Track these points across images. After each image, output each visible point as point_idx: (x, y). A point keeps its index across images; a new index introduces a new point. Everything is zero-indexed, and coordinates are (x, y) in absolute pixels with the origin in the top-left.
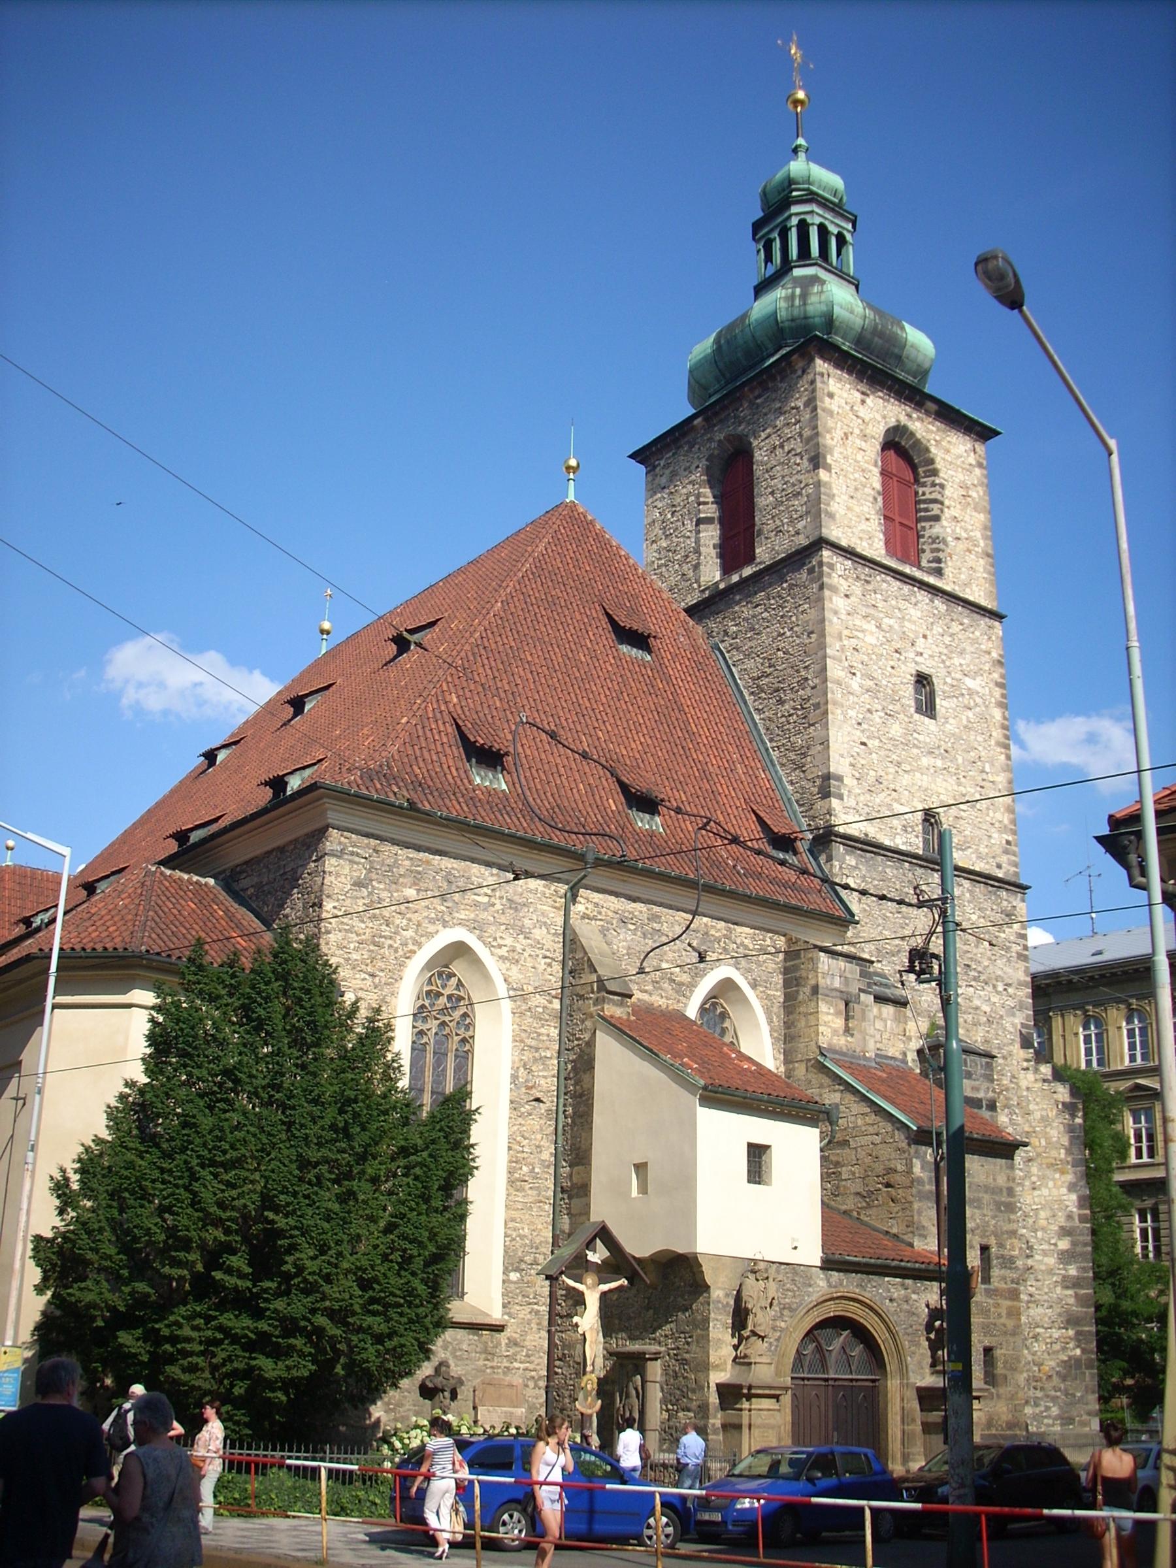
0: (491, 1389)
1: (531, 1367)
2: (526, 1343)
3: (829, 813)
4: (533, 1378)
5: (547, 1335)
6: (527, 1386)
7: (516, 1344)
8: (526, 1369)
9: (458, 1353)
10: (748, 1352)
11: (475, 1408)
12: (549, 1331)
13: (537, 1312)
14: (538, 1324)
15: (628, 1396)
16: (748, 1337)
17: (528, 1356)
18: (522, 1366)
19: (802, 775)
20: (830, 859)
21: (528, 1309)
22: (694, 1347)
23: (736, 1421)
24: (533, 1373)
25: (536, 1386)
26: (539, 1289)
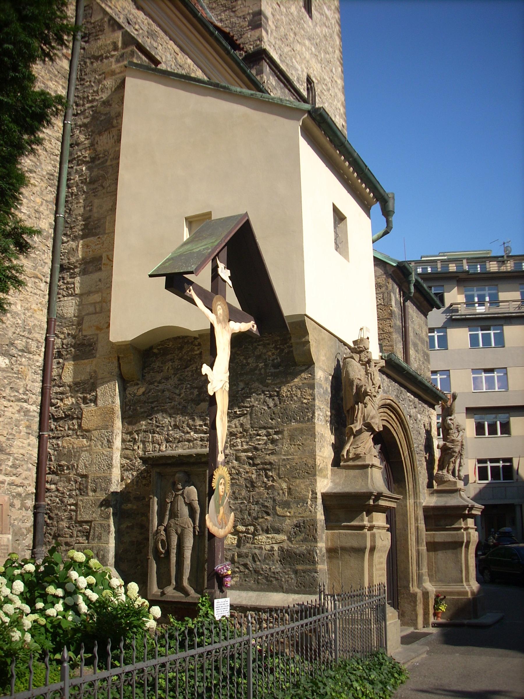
1: (18, 481)
2: (14, 450)
3: (260, 39)
4: (19, 495)
5: (35, 441)
6: (12, 505)
8: (12, 484)
10: (359, 451)
12: (40, 437)
13: (27, 412)
14: (28, 427)
15: (174, 515)
16: (360, 432)
17: (14, 466)
18: (8, 479)
19: (232, 14)
20: (260, 72)
21: (16, 406)
22: (285, 446)
23: (354, 543)
24: (20, 490)
25: (23, 506)
26: (30, 384)
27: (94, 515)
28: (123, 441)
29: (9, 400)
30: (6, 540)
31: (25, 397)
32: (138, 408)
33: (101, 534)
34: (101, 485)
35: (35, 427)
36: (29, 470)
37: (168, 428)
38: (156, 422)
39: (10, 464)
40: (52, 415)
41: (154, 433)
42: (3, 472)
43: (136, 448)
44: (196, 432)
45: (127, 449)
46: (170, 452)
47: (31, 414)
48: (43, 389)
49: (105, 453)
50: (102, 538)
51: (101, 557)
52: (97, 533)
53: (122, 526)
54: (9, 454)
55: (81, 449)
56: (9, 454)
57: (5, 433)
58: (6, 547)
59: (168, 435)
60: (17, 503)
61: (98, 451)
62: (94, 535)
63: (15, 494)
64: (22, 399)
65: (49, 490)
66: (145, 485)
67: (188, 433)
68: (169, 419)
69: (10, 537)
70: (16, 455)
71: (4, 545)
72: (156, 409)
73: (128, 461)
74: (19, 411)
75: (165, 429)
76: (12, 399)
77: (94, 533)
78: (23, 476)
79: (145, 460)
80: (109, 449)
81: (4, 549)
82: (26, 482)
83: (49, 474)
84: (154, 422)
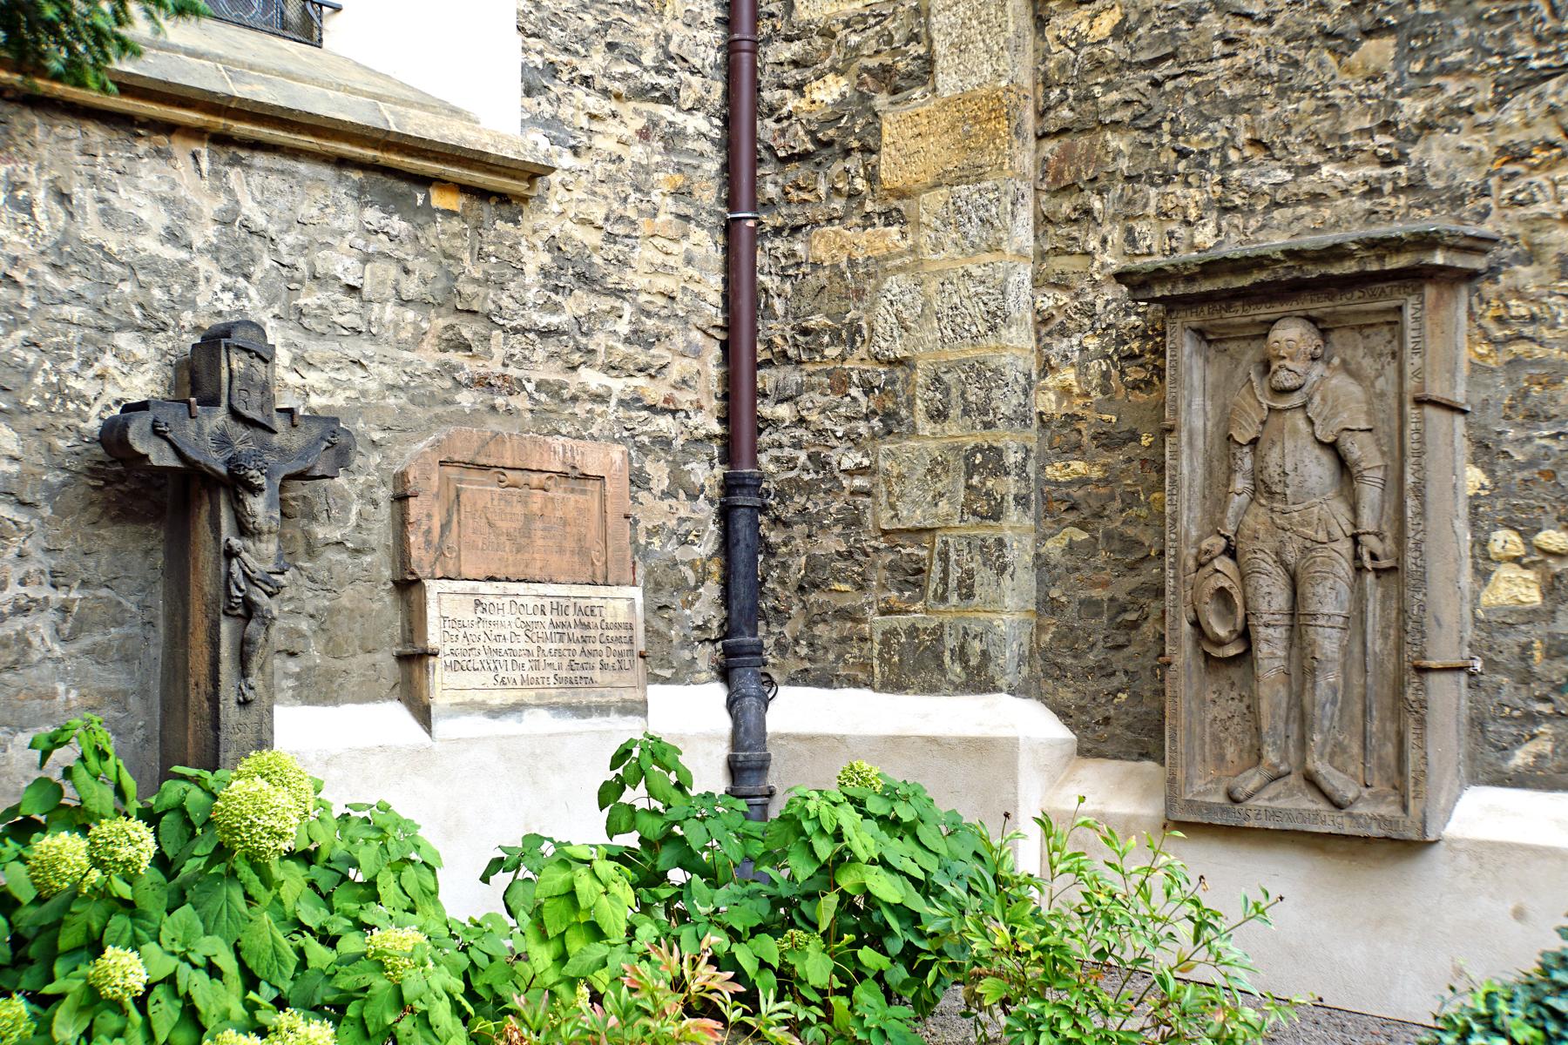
0: (480, 490)
1: (655, 392)
2: (636, 279)
4: (664, 442)
6: (639, 480)
7: (586, 279)
8: (633, 402)
9: (310, 299)
11: (407, 586)
12: (729, 229)
13: (673, 139)
14: (678, 194)
17: (636, 337)
21: (634, 116)
24: (664, 423)
26: (678, 31)
27: (944, 506)
28: (1044, 220)
29: (605, 92)
30: (622, 606)
31: (663, 81)
32: (1097, 90)
33: (970, 574)
34: (963, 393)
35: (709, 195)
36: (697, 353)
37: (1224, 158)
38: (1174, 135)
39: (623, 328)
40: (769, 148)
41: (1167, 182)
42: (600, 358)
43: (1093, 244)
44: (1348, 158)
45: (1056, 251)
46: (1232, 248)
47: (690, 145)
48: (730, 49)
49: (977, 272)
50: (977, 590)
51: (973, 662)
52: (955, 574)
53: (1049, 544)
54: (618, 293)
55: (878, 267)
56: (618, 293)
57: (598, 215)
58: (623, 633)
59: (1223, 183)
60: (658, 472)
61: (948, 265)
62: (944, 580)
63: (646, 440)
64: (654, 87)
65: (774, 423)
66: (1135, 386)
67: (1312, 168)
68: (1226, 120)
69: (637, 593)
70: (643, 298)
71: (617, 626)
72: (1169, 86)
73: (1064, 298)
74: (644, 135)
75: (1214, 162)
76: (616, 86)
77: (945, 571)
78: (674, 374)
79: (1135, 281)
80: (988, 258)
81: (618, 639)
82: (684, 398)
83: (768, 363)
84: (1166, 139)
